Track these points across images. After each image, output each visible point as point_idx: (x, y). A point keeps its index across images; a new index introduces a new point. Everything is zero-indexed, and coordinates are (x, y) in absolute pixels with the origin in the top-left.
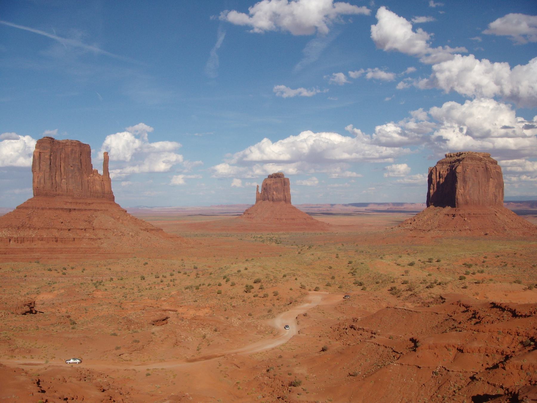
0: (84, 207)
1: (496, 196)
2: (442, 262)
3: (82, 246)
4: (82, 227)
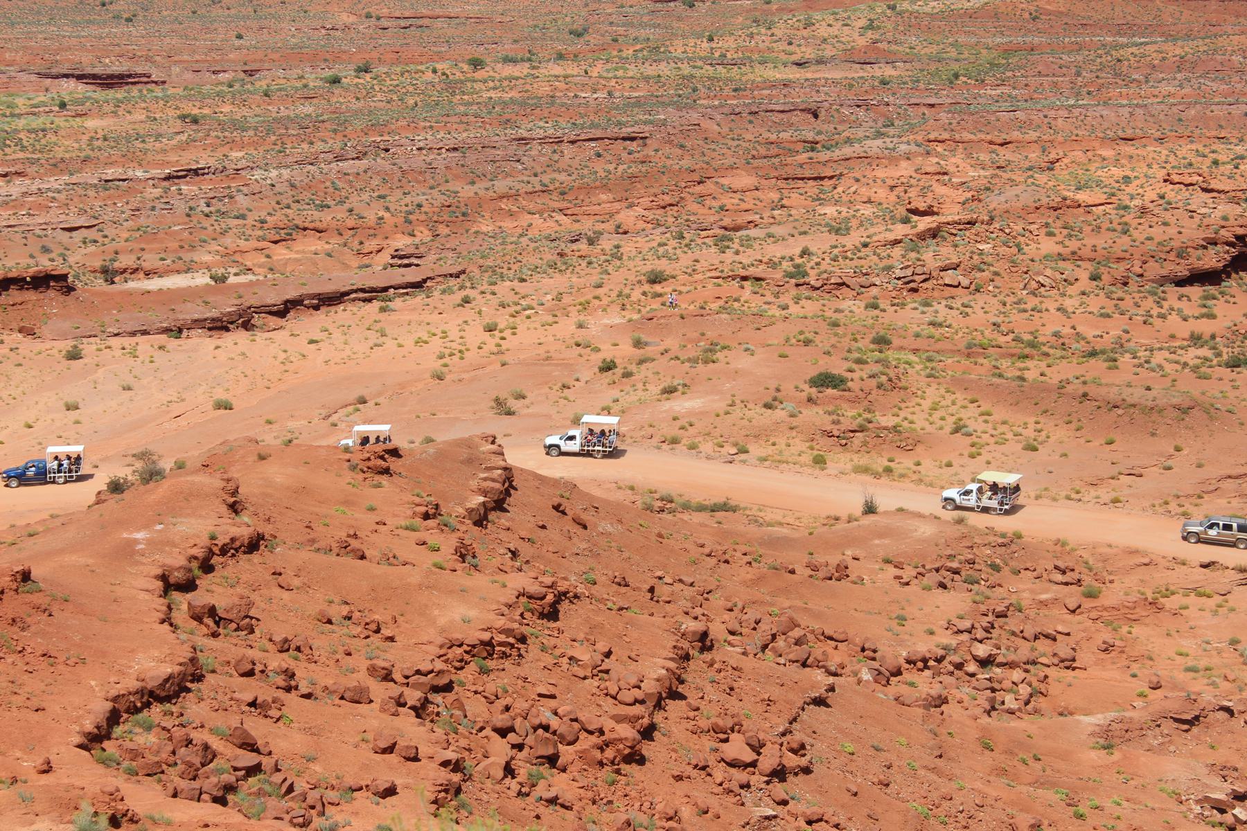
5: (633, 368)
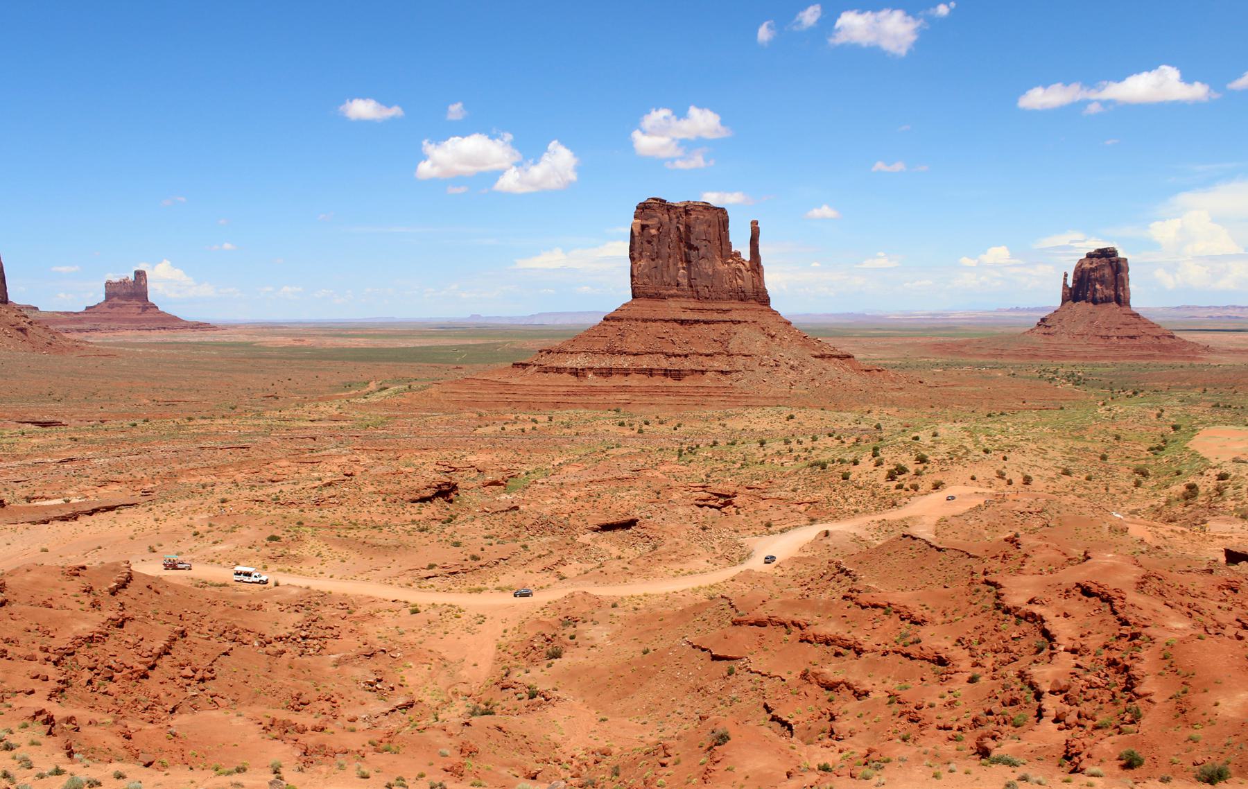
0: (716, 316)
3: (703, 384)
4: (708, 352)
5: (205, 534)
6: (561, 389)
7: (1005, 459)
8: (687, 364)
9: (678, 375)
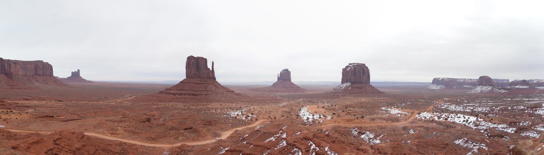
1: (366, 80)
2: (337, 106)
6: (170, 98)
7: (270, 113)
8: (198, 93)
9: (196, 95)
